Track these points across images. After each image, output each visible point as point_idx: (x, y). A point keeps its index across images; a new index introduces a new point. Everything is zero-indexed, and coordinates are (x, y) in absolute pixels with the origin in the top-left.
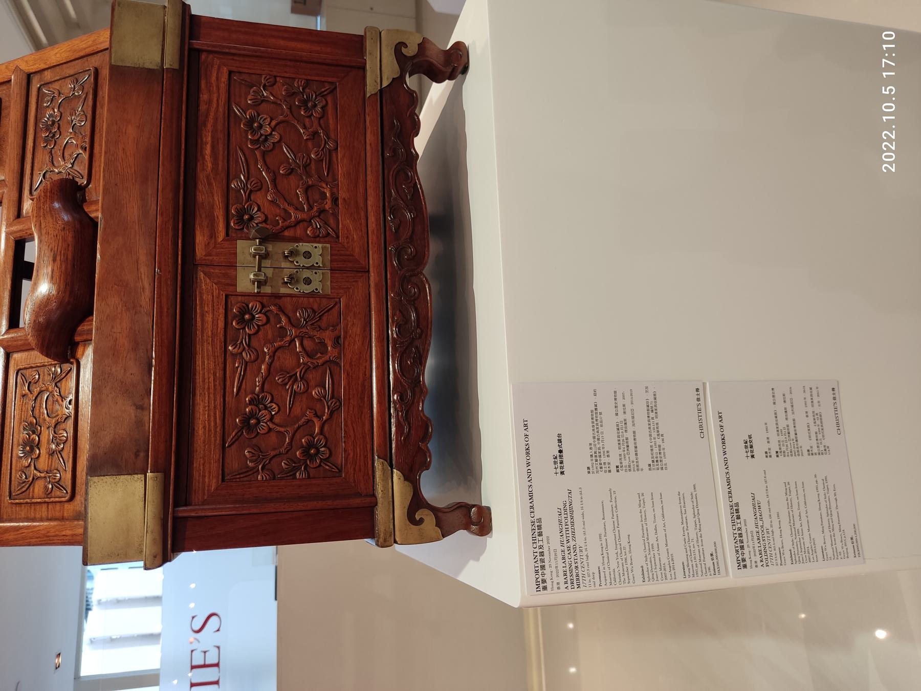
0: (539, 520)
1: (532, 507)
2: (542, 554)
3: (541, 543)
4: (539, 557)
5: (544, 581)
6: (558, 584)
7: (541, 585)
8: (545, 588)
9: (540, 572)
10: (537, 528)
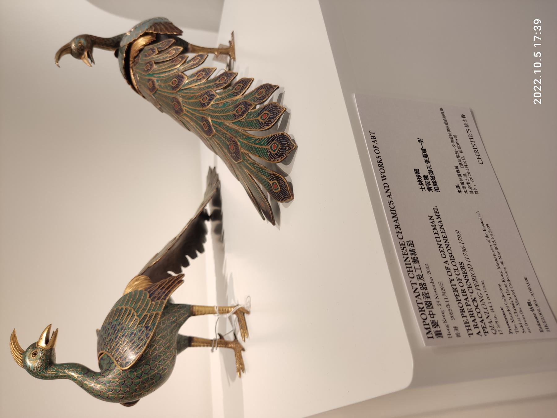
0: (411, 243)
1: (397, 227)
2: (423, 286)
3: (418, 272)
5: (435, 324)
7: (433, 330)
8: (439, 334)
9: (427, 311)
10: (409, 253)
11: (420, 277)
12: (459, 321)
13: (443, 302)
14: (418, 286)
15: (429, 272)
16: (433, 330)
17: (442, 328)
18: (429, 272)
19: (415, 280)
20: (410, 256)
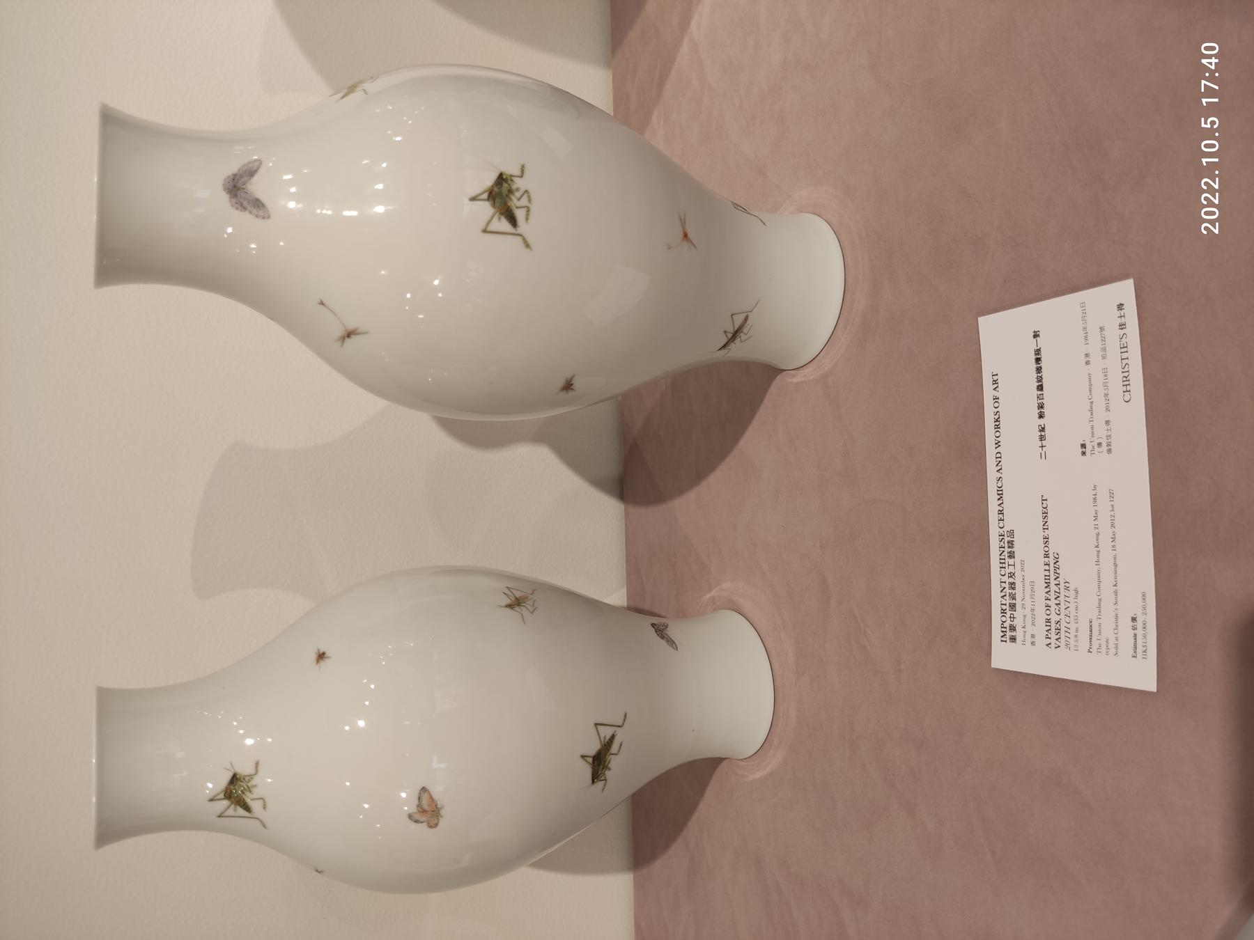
3: (1011, 569)
4: (1007, 591)
5: (1013, 628)
6: (1033, 636)
7: (1009, 634)
8: (1013, 639)
9: (1009, 613)
11: (1012, 575)
12: (1041, 629)
13: (1028, 607)
14: (1007, 585)
15: (1022, 570)
16: (1009, 634)
17: (1019, 634)
18: (1022, 570)
19: (1005, 579)
20: (1007, 550)
